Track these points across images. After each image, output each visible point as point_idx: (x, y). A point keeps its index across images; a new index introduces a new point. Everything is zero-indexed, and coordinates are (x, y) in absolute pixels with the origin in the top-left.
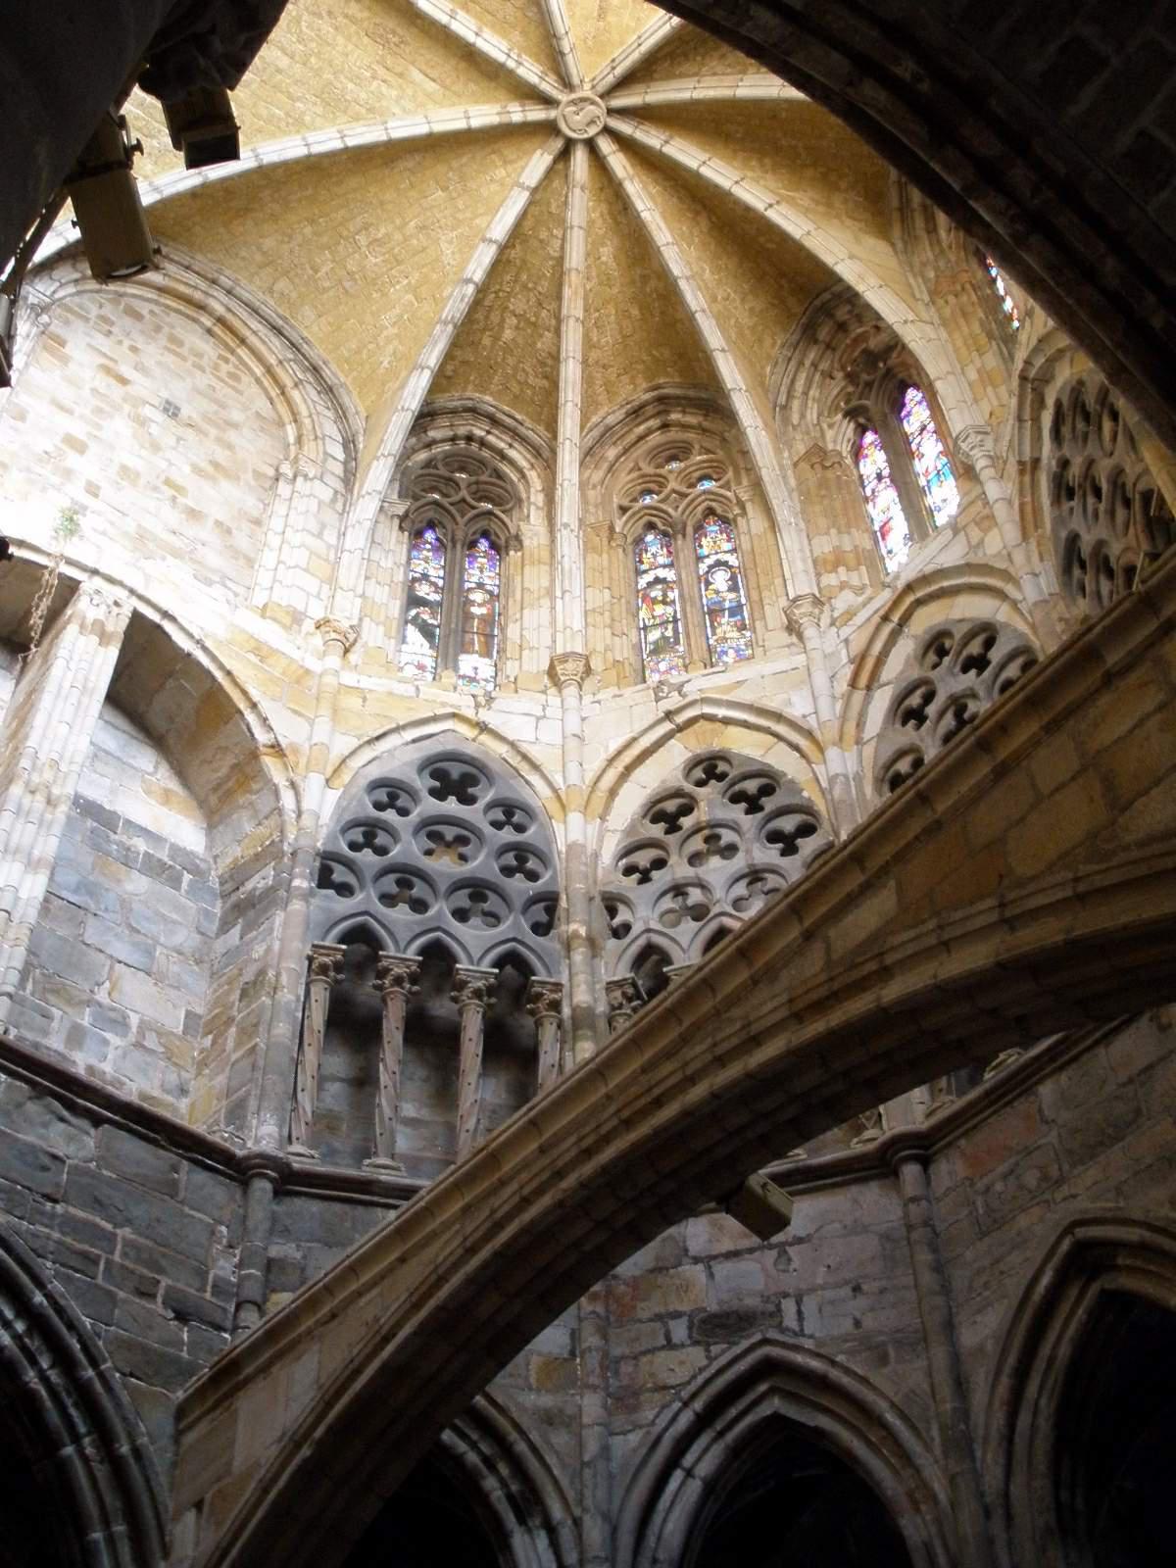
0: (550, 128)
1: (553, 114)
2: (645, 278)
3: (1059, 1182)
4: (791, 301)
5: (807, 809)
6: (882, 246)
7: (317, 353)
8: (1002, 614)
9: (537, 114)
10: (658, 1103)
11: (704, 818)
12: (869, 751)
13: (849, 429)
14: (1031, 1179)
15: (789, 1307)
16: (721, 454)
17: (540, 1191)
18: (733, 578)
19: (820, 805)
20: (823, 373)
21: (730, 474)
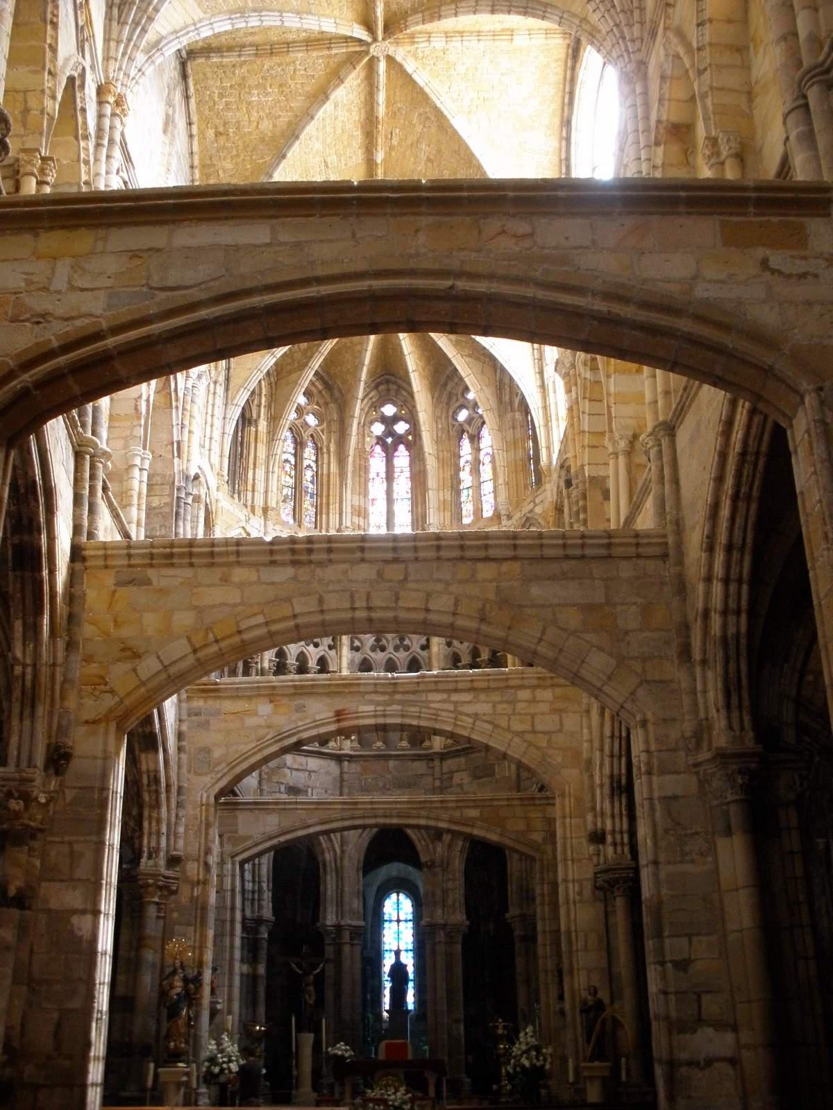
3: (389, 790)
4: (379, 369)
6: (429, 396)
10: (408, 817)
13: (375, 441)
14: (381, 784)
15: (310, 790)
16: (323, 410)
17: (368, 817)
18: (313, 476)
20: (373, 403)
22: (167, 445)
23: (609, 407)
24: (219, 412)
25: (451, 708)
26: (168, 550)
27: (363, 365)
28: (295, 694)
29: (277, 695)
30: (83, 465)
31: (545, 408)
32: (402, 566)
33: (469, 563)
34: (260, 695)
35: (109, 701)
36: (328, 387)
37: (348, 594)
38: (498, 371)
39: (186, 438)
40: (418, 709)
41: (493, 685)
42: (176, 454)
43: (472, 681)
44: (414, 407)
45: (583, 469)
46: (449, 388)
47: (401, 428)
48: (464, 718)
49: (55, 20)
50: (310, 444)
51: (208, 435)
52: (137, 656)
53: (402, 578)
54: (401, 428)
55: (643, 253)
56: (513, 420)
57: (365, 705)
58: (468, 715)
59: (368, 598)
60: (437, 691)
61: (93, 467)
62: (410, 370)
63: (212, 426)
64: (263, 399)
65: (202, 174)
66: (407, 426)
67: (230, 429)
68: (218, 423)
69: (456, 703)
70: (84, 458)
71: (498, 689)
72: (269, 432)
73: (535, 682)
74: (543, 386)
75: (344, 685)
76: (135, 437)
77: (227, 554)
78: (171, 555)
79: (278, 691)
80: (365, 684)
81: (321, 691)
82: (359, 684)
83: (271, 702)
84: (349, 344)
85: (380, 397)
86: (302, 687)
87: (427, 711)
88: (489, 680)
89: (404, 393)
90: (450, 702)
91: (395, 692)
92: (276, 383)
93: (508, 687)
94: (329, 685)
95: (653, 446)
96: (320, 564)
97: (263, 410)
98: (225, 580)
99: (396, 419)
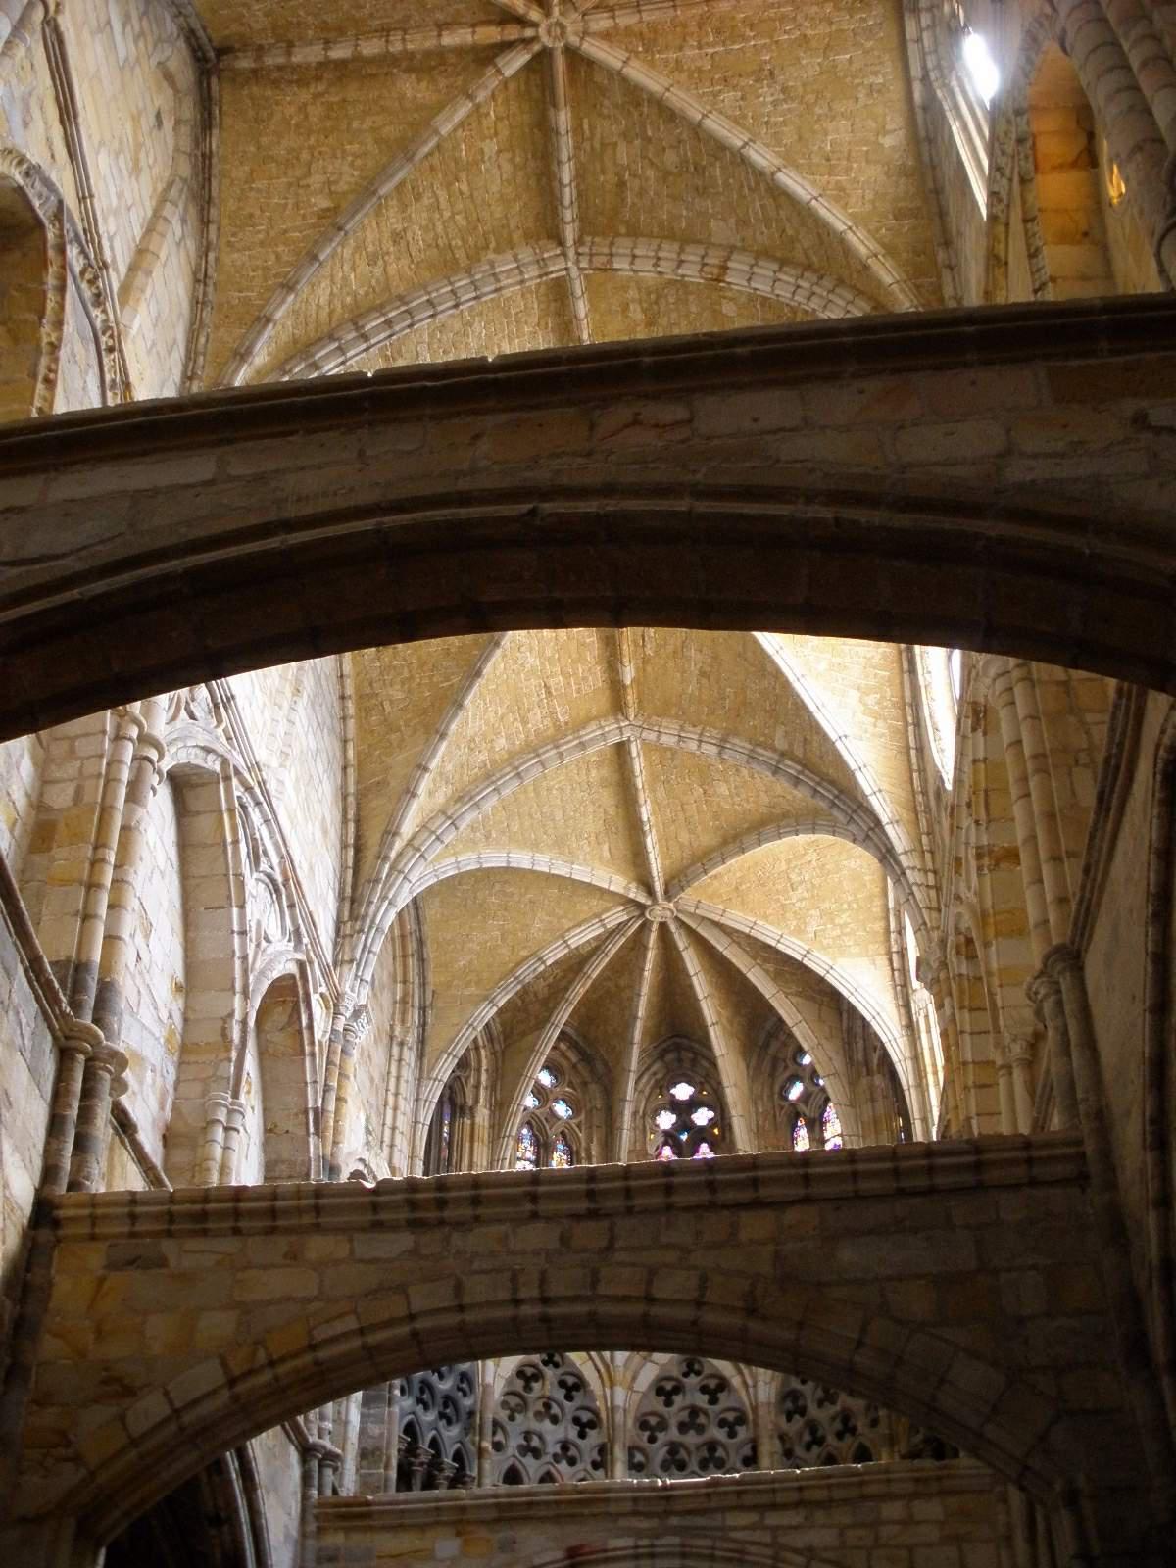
0: (641, 907)
1: (649, 902)
2: (608, 979)
5: (596, 1413)
6: (742, 1066)
7: (428, 930)
8: (736, 1381)
9: (642, 898)
11: (547, 1393)
12: (636, 1397)
19: (603, 1415)
20: (657, 1081)
21: (582, 1117)
22: (296, 1115)
23: (991, 994)
24: (407, 1089)
25: (767, 1538)
26: (198, 1207)
27: (635, 1018)
28: (497, 1521)
29: (469, 1522)
30: (71, 1070)
31: (917, 1058)
32: (605, 1224)
33: (726, 1213)
34: (438, 1523)
35: (70, 1476)
36: (586, 1058)
37: (508, 1275)
38: (845, 1016)
39: (332, 1107)
40: (708, 1542)
41: (838, 1494)
42: (312, 1130)
43: (800, 1489)
44: (720, 1083)
45: (970, 1127)
46: (772, 1050)
47: (702, 1117)
48: (789, 1556)
49: (52, 376)
50: (560, 1146)
51: (389, 1121)
52: (129, 1391)
53: (604, 1243)
54: (702, 1117)
55: (901, 428)
56: (872, 1087)
57: (618, 1536)
58: (796, 1551)
59: (543, 1280)
60: (742, 1508)
61: (90, 1076)
62: (709, 1023)
63: (395, 1109)
64: (484, 1077)
65: (359, 709)
66: (711, 1114)
67: (427, 1116)
68: (406, 1107)
69: (775, 1529)
70: (73, 1059)
71: (846, 1501)
72: (492, 1126)
73: (910, 1487)
74: (911, 1027)
75: (580, 1502)
76: (223, 1078)
77: (299, 1211)
78: (204, 1216)
79: (472, 1516)
80: (617, 1500)
81: (543, 1513)
82: (607, 1500)
83: (458, 1534)
84: (613, 989)
85: (669, 1071)
86: (511, 1506)
87: (726, 1545)
88: (829, 1487)
89: (705, 1064)
90: (765, 1528)
91: (668, 1513)
92: (503, 1052)
93: (864, 1498)
94: (557, 1503)
95: (1046, 996)
96: (459, 1225)
97: (482, 1093)
98: (293, 1257)
99: (693, 1105)
